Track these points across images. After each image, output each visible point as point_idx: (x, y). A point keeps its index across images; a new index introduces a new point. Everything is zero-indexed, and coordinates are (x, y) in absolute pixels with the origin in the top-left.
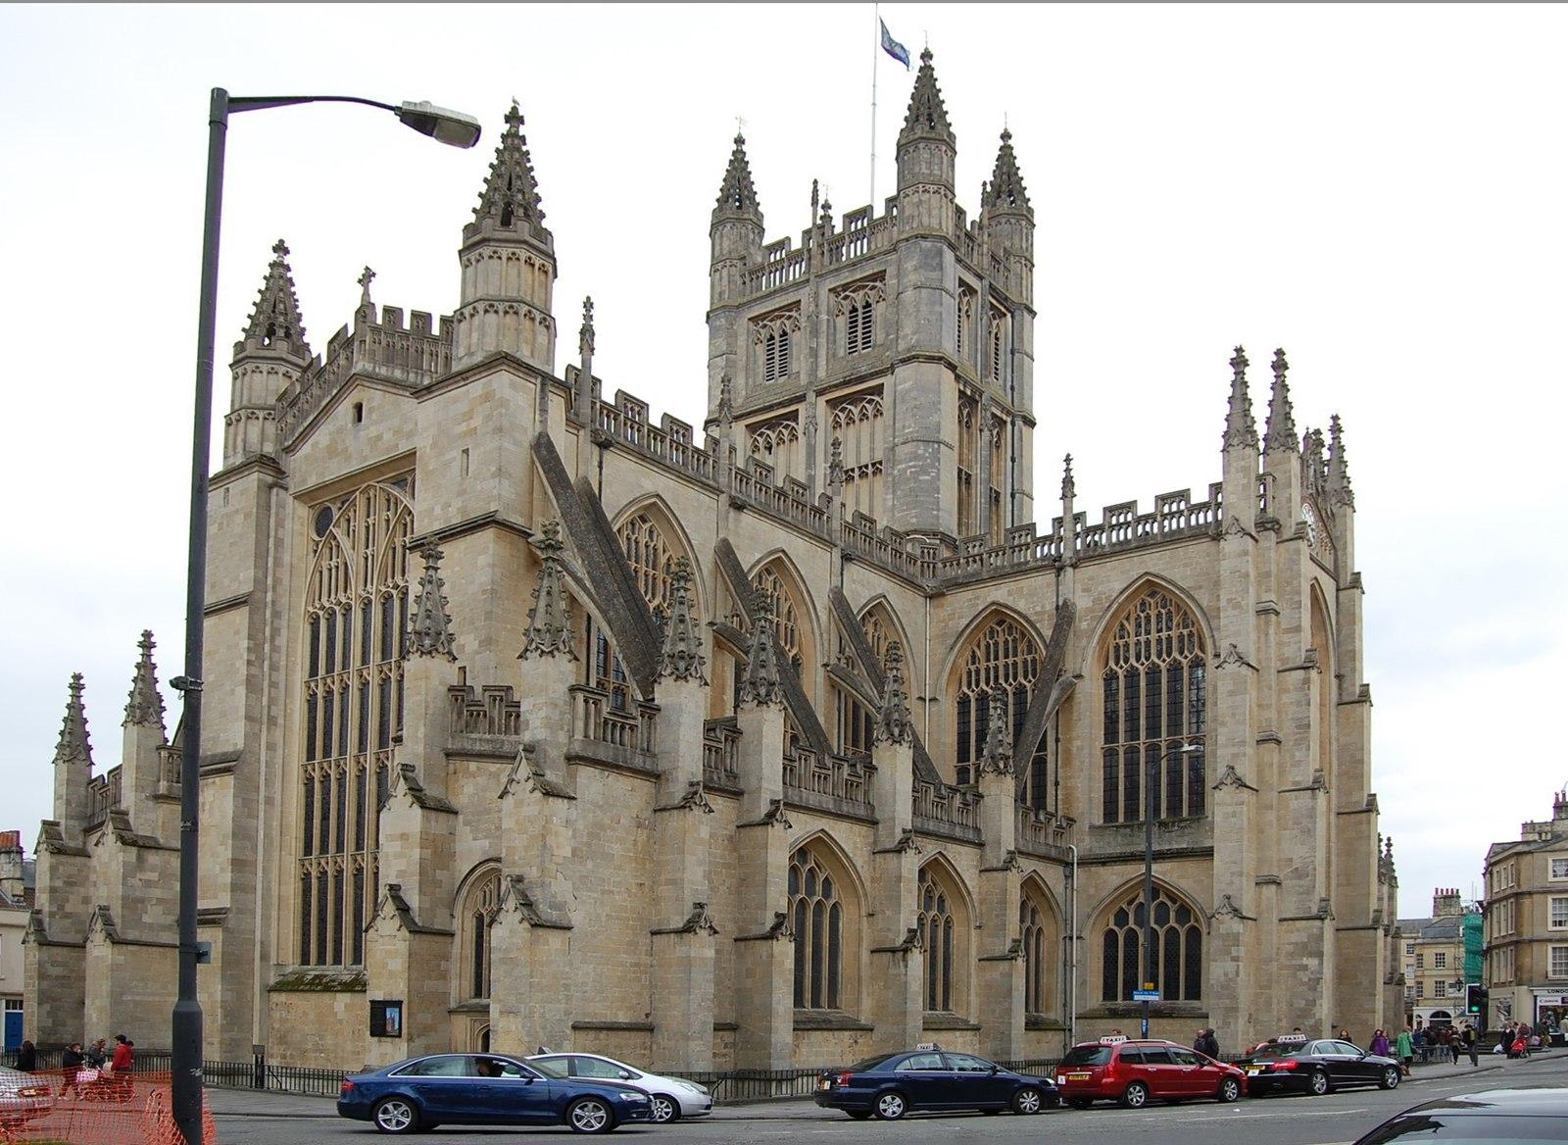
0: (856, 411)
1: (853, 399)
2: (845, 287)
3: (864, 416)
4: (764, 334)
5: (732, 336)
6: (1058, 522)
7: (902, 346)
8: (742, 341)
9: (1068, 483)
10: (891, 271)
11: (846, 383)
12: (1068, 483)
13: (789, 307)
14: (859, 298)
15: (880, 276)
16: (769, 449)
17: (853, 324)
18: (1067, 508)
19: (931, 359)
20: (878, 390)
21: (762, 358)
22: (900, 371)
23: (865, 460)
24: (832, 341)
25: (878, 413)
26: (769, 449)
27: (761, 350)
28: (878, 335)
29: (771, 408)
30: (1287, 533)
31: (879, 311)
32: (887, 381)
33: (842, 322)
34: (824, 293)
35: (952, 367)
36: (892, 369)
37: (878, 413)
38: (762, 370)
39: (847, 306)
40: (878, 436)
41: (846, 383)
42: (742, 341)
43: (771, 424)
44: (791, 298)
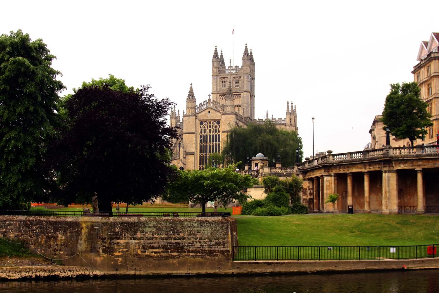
0: (237, 96)
1: (237, 95)
2: (235, 77)
3: (238, 98)
4: (222, 81)
5: (217, 80)
6: (266, 119)
7: (244, 89)
8: (218, 81)
9: (267, 114)
10: (242, 78)
11: (235, 92)
12: (267, 114)
13: (226, 78)
14: (237, 79)
15: (240, 77)
16: (223, 99)
17: (236, 83)
18: (267, 118)
19: (248, 92)
20: (240, 94)
21: (221, 84)
22: (244, 93)
23: (238, 104)
24: (233, 85)
25: (240, 98)
26: (223, 99)
27: (221, 83)
28: (240, 86)
29: (223, 93)
30: (293, 126)
31: (240, 82)
32: (242, 94)
33: (234, 82)
34: (232, 77)
35: (250, 92)
36: (243, 92)
37: (240, 98)
38: (221, 86)
39: (235, 80)
40: (240, 101)
41: (235, 92)
42: (218, 81)
43: (223, 95)
44: (226, 76)
